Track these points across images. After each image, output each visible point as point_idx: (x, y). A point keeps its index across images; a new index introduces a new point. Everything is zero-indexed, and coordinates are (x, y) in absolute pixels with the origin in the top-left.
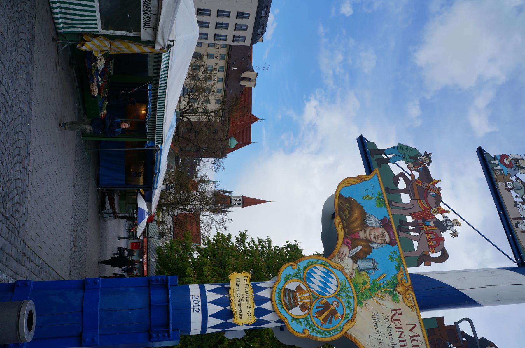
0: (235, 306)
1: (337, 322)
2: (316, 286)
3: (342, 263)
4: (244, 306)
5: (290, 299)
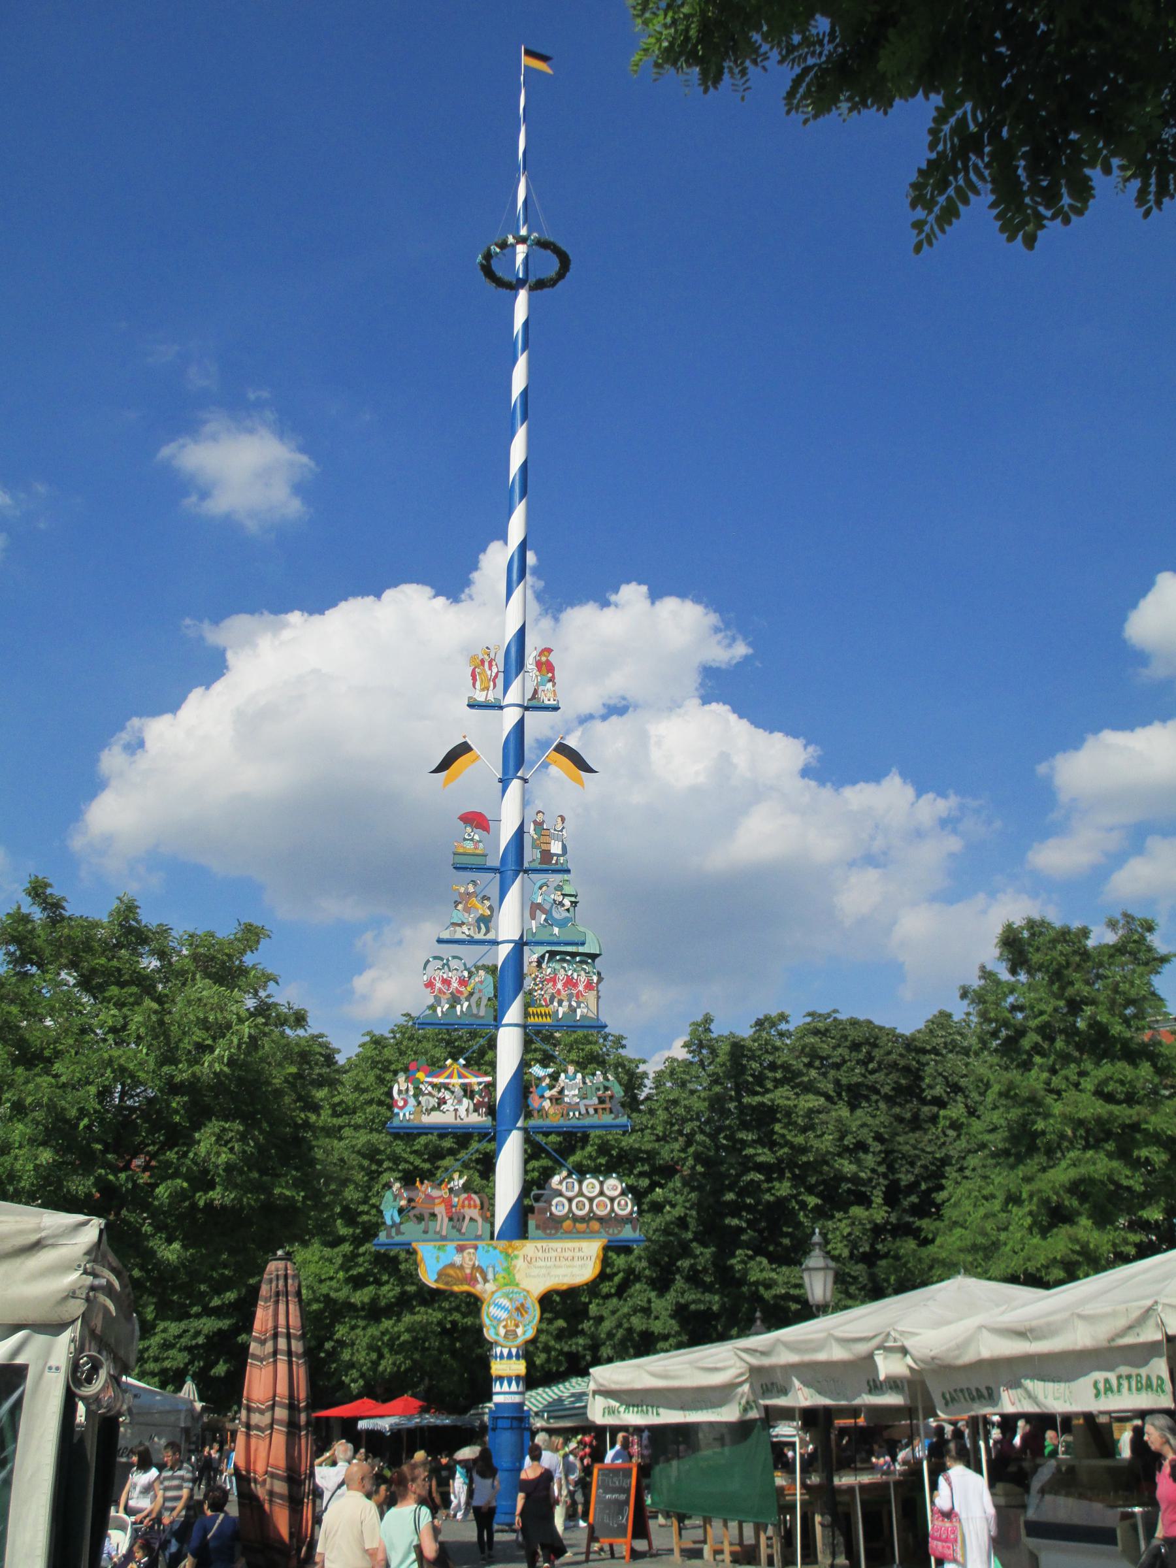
0: (513, 1373)
1: (529, 1304)
2: (503, 1315)
3: (489, 1291)
4: (515, 1367)
5: (511, 1334)
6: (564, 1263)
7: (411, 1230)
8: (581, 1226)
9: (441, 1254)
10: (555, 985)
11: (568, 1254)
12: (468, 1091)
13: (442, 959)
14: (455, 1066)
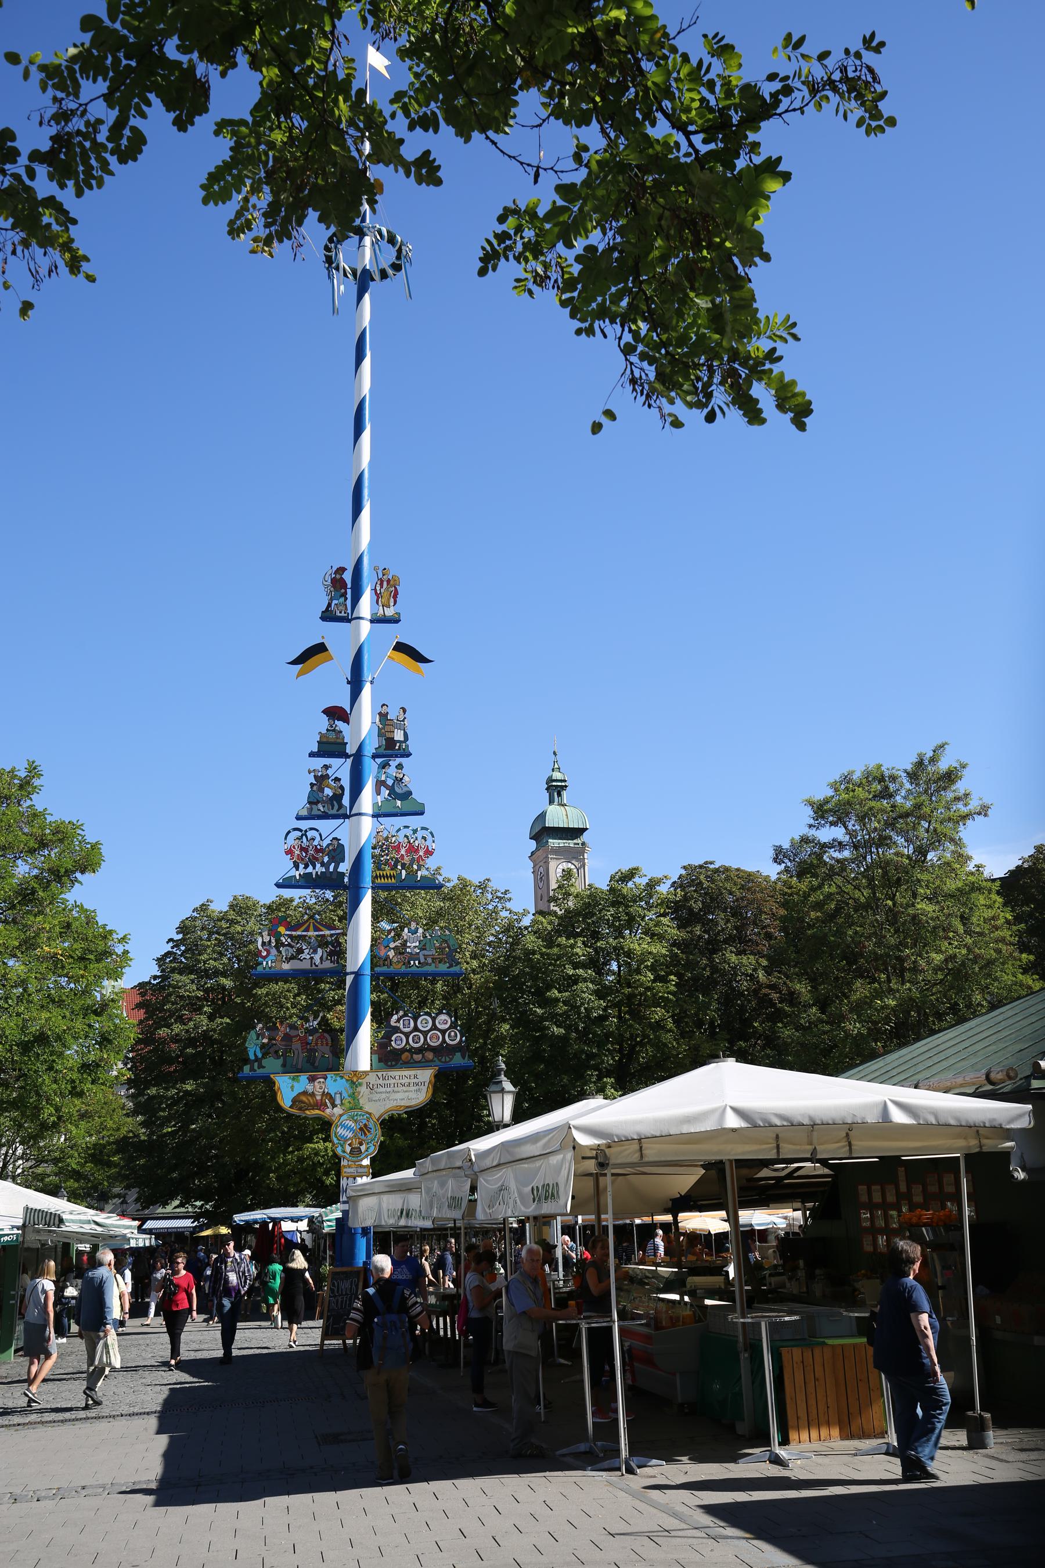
1: (371, 1125)
6: (401, 1088)
7: (271, 1064)
8: (418, 1057)
9: (296, 1084)
10: (398, 851)
11: (405, 1081)
12: (322, 942)
13: (300, 830)
14: (311, 921)
